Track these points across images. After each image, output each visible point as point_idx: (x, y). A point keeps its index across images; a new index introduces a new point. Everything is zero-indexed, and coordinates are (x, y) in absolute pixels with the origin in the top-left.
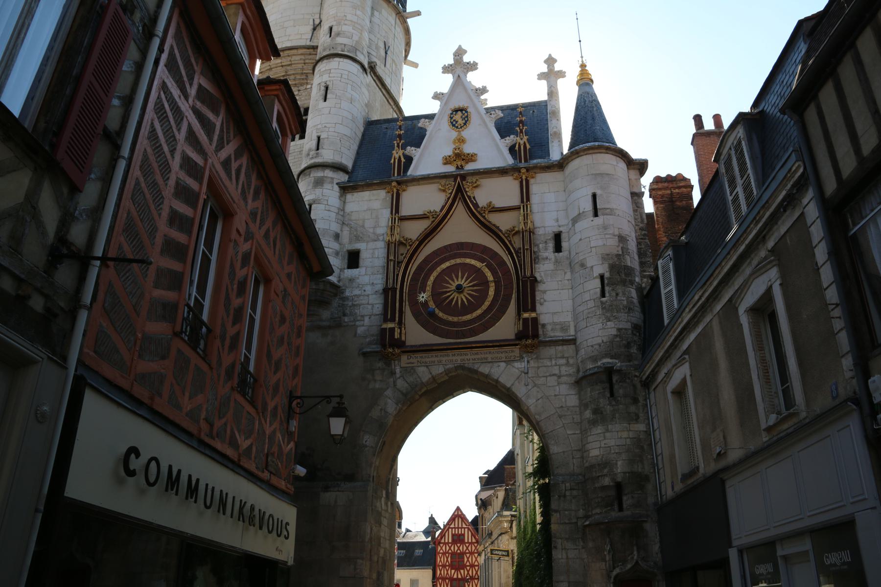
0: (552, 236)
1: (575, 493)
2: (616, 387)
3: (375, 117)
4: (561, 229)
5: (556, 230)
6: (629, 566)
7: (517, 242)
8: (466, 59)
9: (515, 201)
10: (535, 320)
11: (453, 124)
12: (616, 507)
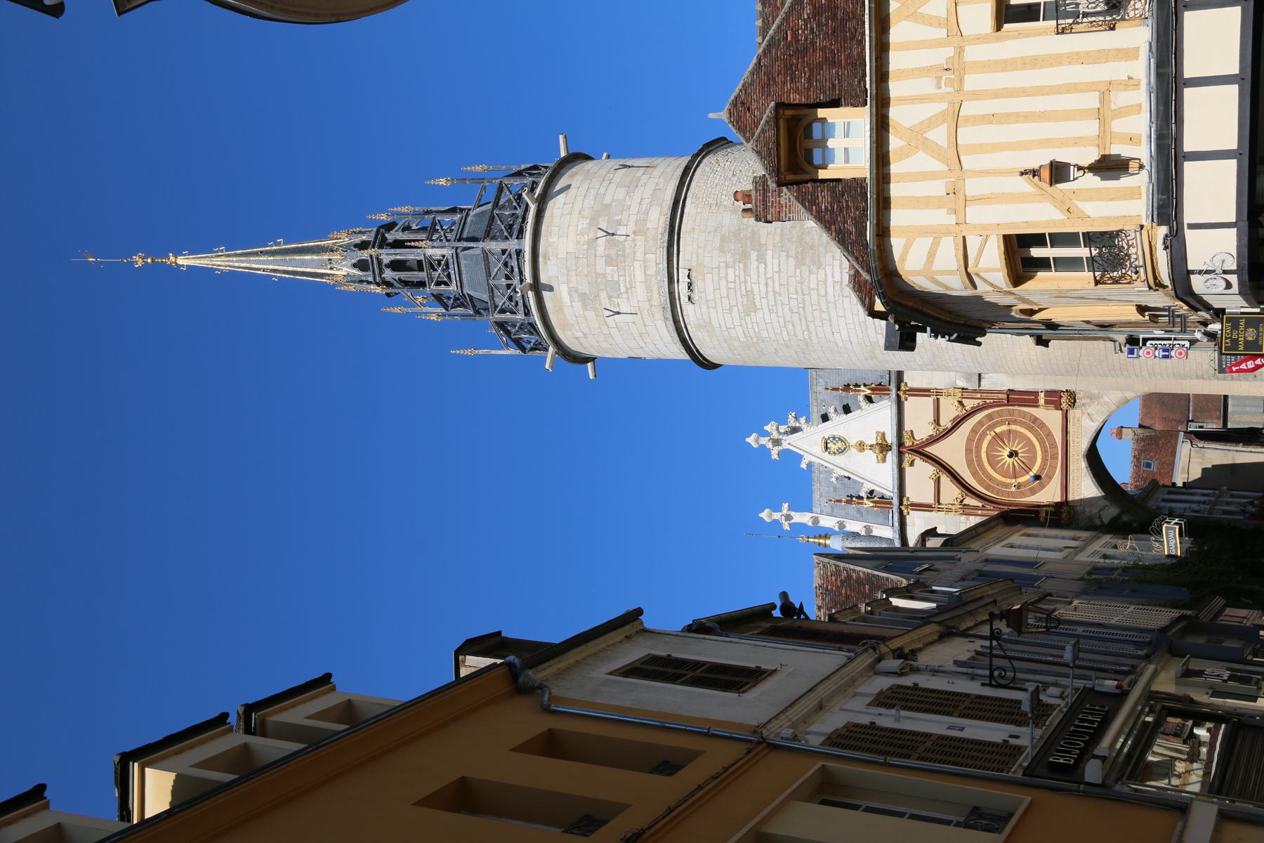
7: (970, 404)
9: (929, 401)
10: (1049, 393)
11: (841, 451)
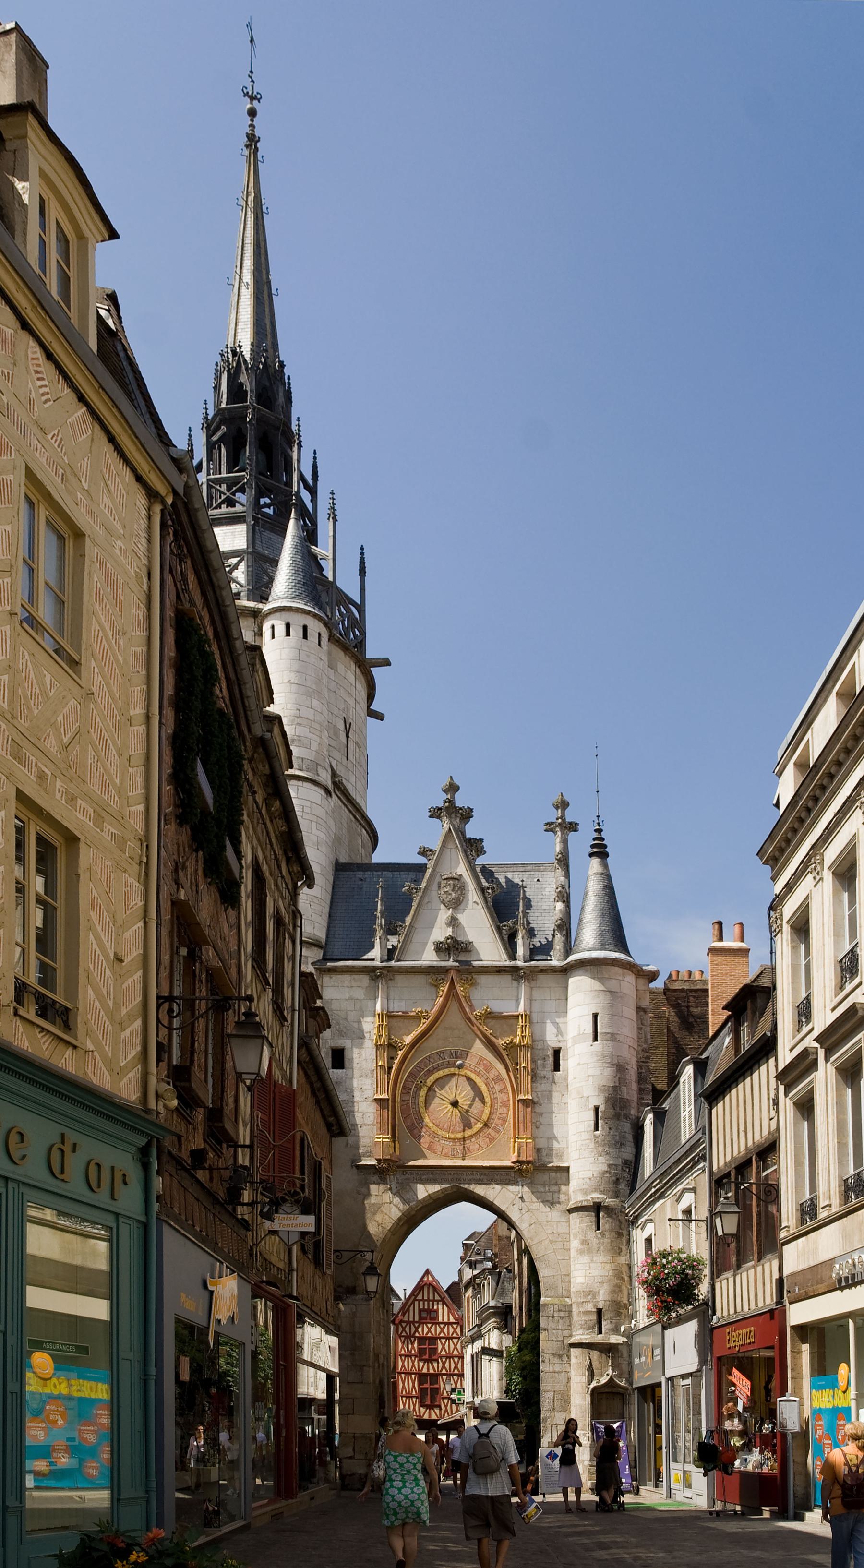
0: (550, 1053)
1: (562, 1314)
2: (601, 1221)
3: (343, 860)
4: (560, 1045)
5: (556, 1045)
6: (604, 1380)
8: (461, 801)
12: (596, 1330)
